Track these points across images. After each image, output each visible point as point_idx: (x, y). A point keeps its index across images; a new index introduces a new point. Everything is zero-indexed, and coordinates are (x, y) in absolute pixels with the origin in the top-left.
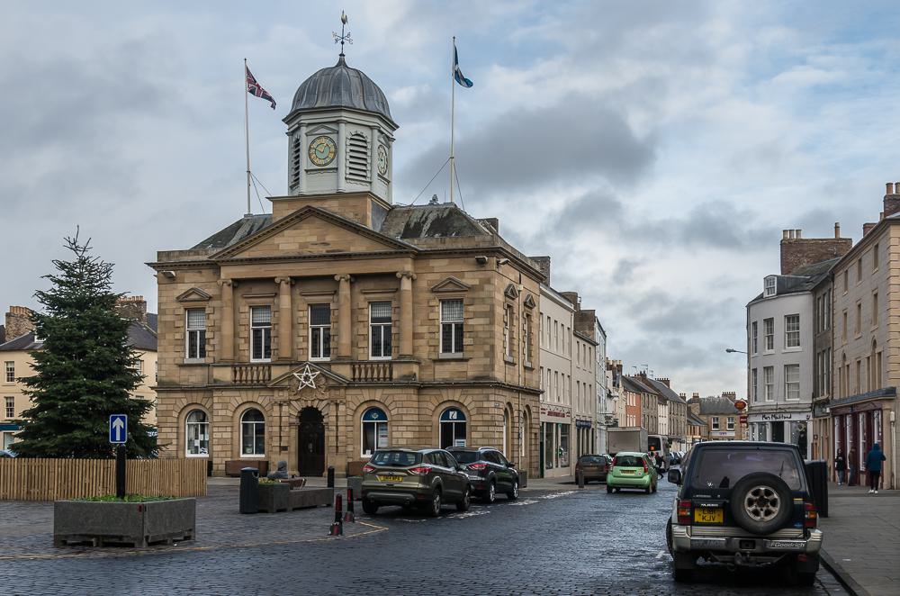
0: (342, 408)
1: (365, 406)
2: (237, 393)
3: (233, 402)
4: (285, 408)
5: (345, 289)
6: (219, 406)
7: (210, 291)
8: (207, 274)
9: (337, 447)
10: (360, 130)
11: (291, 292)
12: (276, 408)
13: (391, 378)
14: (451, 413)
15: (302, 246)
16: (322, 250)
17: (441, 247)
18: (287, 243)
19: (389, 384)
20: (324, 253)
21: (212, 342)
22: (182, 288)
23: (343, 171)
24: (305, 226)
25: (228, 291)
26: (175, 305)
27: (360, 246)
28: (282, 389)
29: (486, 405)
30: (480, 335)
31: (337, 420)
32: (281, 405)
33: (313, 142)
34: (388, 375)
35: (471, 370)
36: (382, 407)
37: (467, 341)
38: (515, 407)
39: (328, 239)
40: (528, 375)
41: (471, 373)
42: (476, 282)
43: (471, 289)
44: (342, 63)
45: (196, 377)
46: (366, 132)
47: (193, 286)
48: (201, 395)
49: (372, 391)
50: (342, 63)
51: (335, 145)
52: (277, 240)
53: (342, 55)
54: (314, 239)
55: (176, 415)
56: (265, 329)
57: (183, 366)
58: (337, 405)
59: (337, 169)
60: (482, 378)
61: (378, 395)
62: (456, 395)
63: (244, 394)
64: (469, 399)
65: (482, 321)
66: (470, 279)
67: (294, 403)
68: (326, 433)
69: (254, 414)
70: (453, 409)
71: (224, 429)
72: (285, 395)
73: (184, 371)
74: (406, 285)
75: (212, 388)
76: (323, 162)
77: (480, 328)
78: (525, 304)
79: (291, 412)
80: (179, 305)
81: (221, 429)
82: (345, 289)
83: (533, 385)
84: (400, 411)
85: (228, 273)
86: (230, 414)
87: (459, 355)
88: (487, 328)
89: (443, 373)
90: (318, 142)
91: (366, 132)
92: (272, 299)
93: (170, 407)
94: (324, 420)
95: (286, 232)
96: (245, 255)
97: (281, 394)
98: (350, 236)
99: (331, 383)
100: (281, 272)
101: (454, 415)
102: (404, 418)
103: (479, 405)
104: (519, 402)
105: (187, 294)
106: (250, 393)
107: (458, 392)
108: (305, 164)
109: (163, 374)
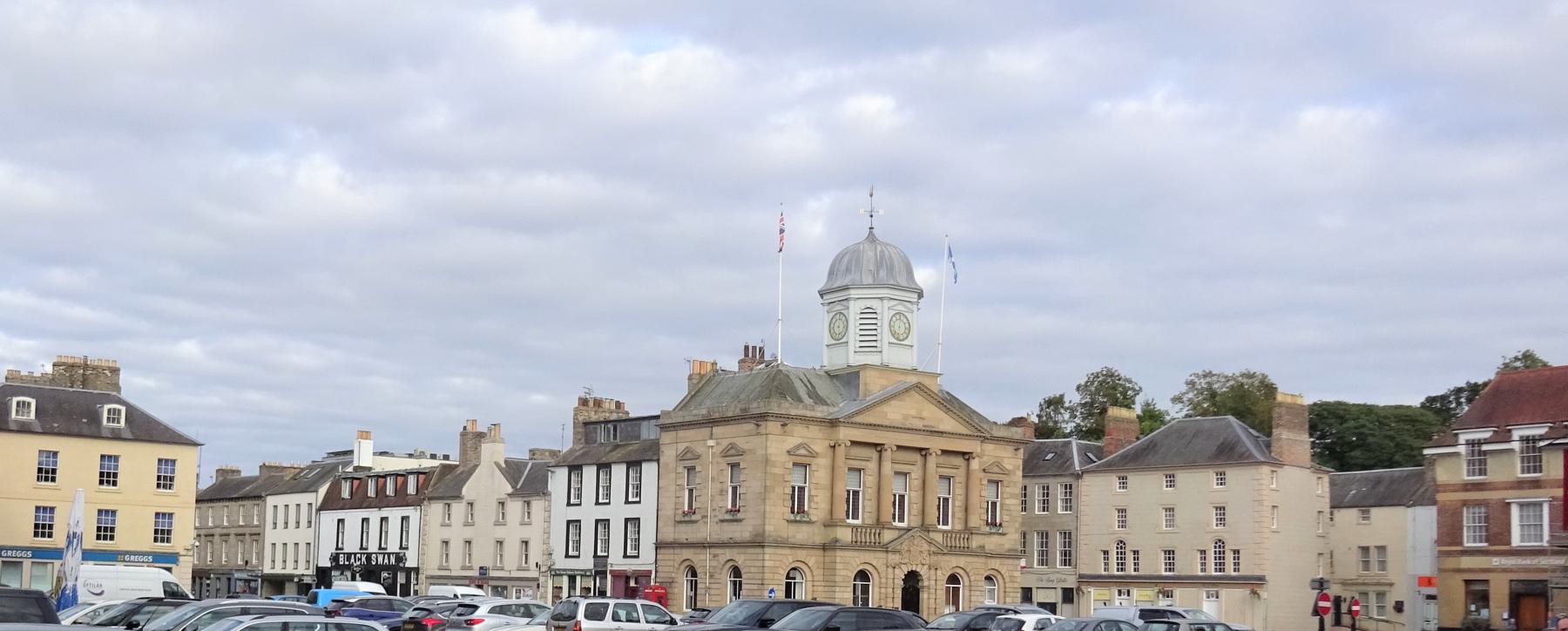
15: (906, 417)
16: (919, 424)
18: (894, 413)
19: (966, 551)
26: (785, 458)
27: (948, 423)
39: (925, 414)
41: (1007, 546)
45: (802, 534)
47: (800, 441)
48: (804, 552)
50: (871, 237)
52: (885, 408)
54: (913, 412)
61: (962, 561)
73: (793, 527)
79: (900, 574)
82: (932, 461)
85: (846, 434)
96: (859, 419)
98: (941, 414)
100: (890, 439)
105: (798, 447)
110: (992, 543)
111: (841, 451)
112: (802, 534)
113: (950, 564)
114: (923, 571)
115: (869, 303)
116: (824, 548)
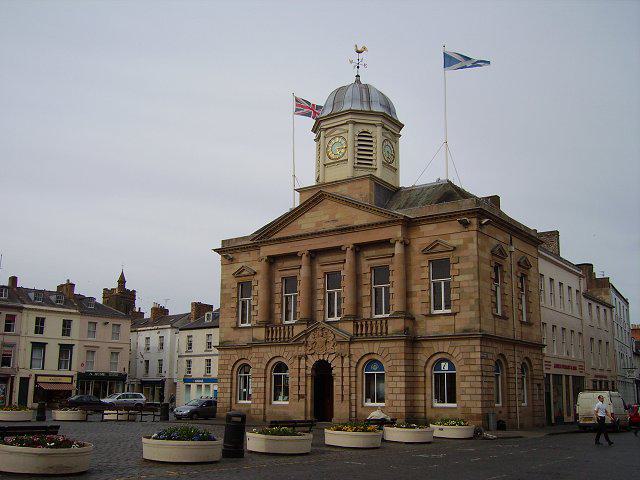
1: (366, 359)
6: (256, 360)
10: (365, 128)
11: (311, 262)
13: (386, 333)
14: (443, 364)
15: (318, 224)
16: (332, 226)
18: (306, 224)
22: (237, 267)
23: (350, 165)
28: (300, 345)
29: (472, 356)
32: (300, 359)
37: (454, 296)
38: (510, 359)
39: (337, 217)
40: (525, 329)
42: (461, 242)
44: (358, 81)
46: (370, 129)
50: (358, 81)
54: (327, 218)
55: (230, 368)
56: (381, 313)
57: (236, 328)
61: (376, 347)
62: (445, 346)
64: (458, 351)
69: (281, 367)
70: (444, 360)
72: (302, 350)
73: (237, 333)
75: (254, 344)
78: (519, 264)
83: (534, 339)
87: (449, 311)
89: (431, 327)
91: (370, 129)
96: (275, 237)
101: (445, 366)
103: (466, 356)
104: (515, 358)
106: (278, 349)
107: (448, 344)
113: (361, 349)
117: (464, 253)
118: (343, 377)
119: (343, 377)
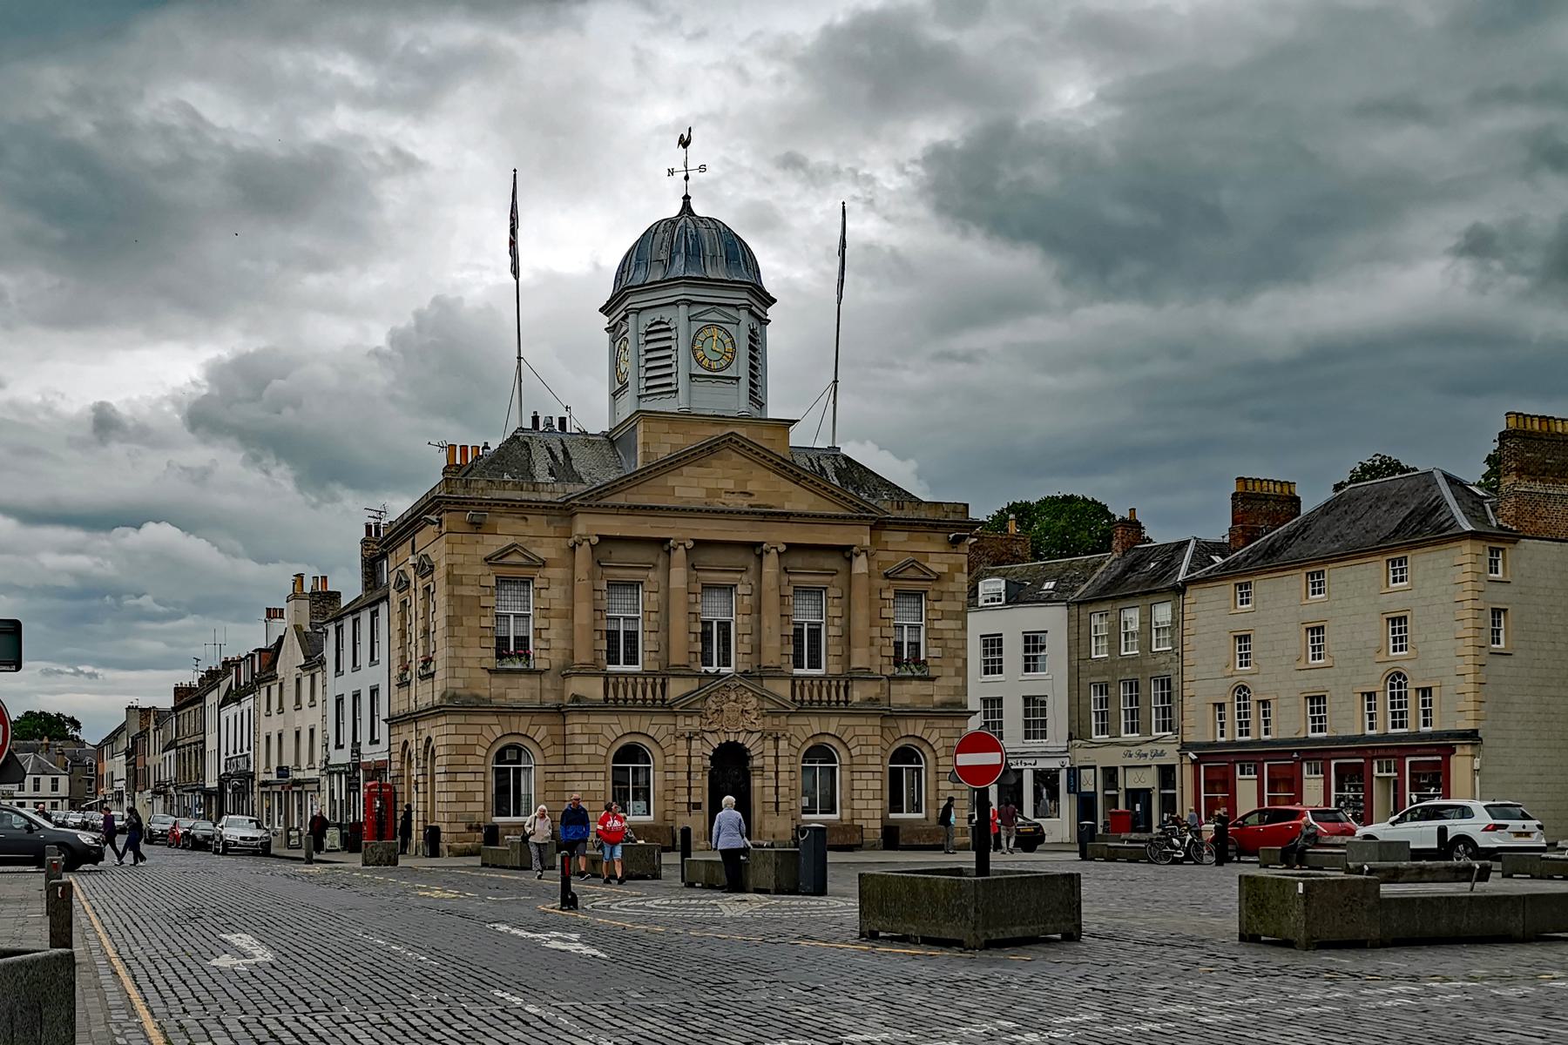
0: (783, 744)
1: (811, 743)
2: (614, 719)
3: (607, 731)
4: (695, 744)
5: (771, 565)
6: (585, 739)
7: (545, 551)
8: (537, 524)
9: (777, 803)
12: (682, 743)
13: (846, 702)
15: (712, 493)
16: (743, 503)
17: (897, 514)
18: (688, 487)
19: (844, 708)
20: (745, 507)
21: (544, 634)
22: (492, 544)
24: (715, 463)
25: (583, 553)
27: (800, 500)
28: (690, 715)
30: (951, 644)
31: (777, 763)
32: (690, 739)
33: (700, 331)
34: (842, 697)
35: (938, 693)
36: (835, 743)
39: (750, 488)
41: (937, 699)
42: (945, 569)
43: (939, 577)
45: (520, 691)
47: (510, 540)
48: (526, 720)
49: (824, 720)
51: (732, 342)
52: (671, 480)
53: (687, 198)
54: (730, 485)
55: (481, 752)
58: (777, 739)
59: (738, 379)
60: (953, 704)
61: (833, 725)
62: (917, 727)
63: (625, 720)
65: (952, 624)
66: (937, 565)
67: (708, 736)
68: (756, 782)
71: (592, 776)
72: (695, 723)
73: (498, 681)
74: (860, 565)
76: (715, 365)
77: (950, 635)
79: (703, 750)
80: (486, 569)
81: (586, 776)
82: (771, 565)
84: (865, 750)
85: (587, 526)
86: (603, 752)
88: (959, 634)
89: (905, 694)
90: (707, 332)
92: (644, 573)
93: (472, 740)
94: (756, 762)
95: (685, 469)
96: (619, 499)
97: (688, 721)
98: (787, 486)
99: (767, 706)
102: (870, 761)
105: (505, 552)
106: (635, 720)
107: (921, 723)
108: (683, 364)
109: (459, 683)
110: (905, 694)
111: (583, 553)
112: (520, 691)
113: (809, 728)
114: (750, 742)
115: (657, 315)
116: (560, 712)
117: (952, 587)
118: (777, 773)
119: (777, 773)
